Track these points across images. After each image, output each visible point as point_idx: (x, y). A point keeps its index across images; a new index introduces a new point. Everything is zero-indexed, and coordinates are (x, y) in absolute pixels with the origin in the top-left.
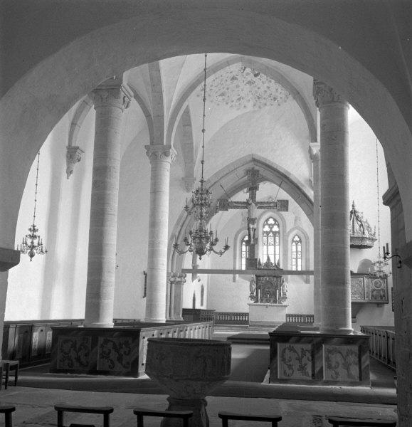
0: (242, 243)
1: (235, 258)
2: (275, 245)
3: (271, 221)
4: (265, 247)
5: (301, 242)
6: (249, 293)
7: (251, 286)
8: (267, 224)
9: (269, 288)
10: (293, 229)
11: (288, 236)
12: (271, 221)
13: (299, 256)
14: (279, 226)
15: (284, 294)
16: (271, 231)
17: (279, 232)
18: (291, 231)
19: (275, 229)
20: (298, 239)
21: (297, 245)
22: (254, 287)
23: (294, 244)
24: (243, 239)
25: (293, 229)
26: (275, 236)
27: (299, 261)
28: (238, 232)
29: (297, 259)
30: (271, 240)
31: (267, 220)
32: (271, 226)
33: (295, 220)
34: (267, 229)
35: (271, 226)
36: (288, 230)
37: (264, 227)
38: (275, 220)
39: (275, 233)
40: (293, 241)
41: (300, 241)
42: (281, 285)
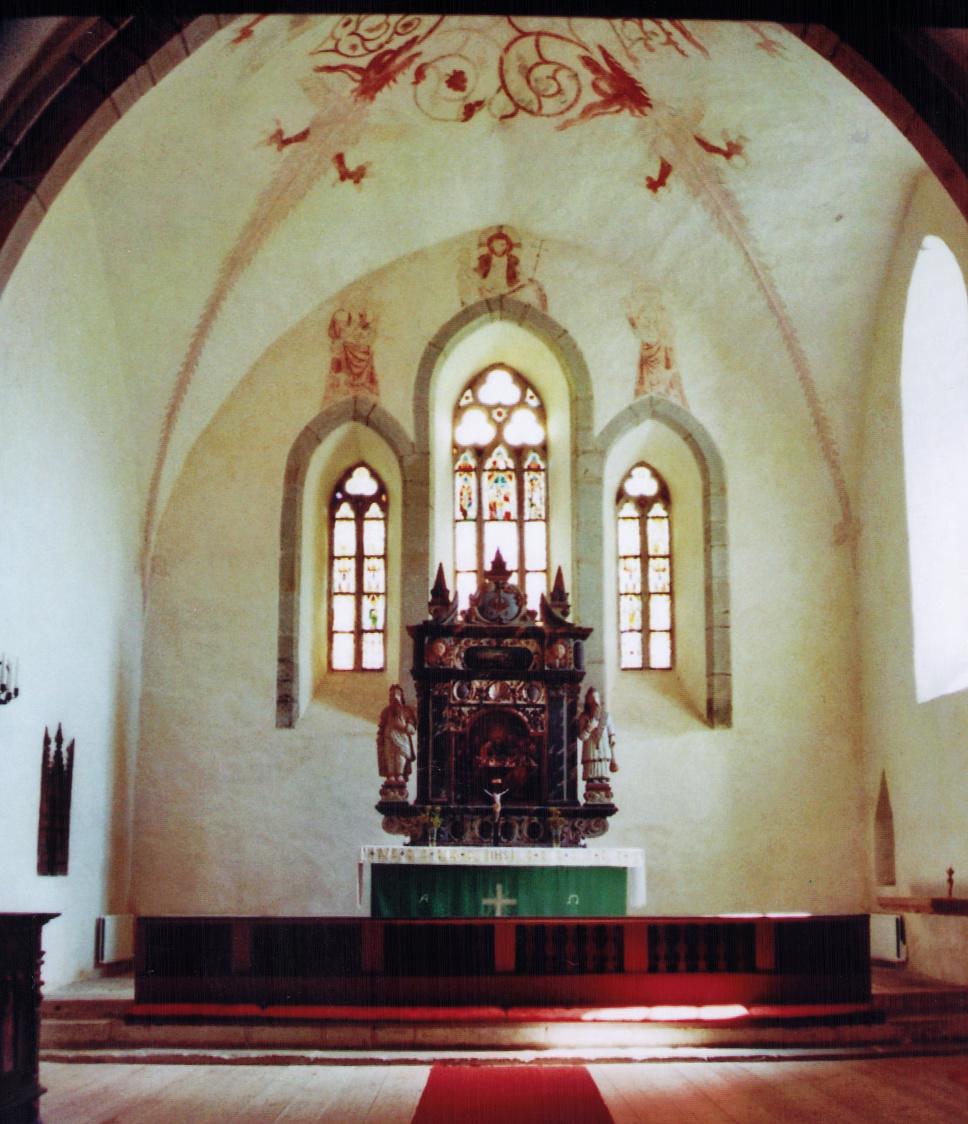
0: (334, 505)
1: (289, 581)
2: (521, 523)
3: (500, 388)
4: (468, 530)
5: (664, 495)
6: (372, 785)
7: (383, 740)
8: (477, 403)
9: (501, 751)
10: (632, 415)
11: (602, 454)
12: (500, 388)
13: (658, 580)
14: (542, 412)
15: (598, 785)
16: (498, 441)
17: (543, 449)
18: (614, 429)
19: (524, 429)
20: (650, 488)
21: (643, 520)
22: (408, 743)
23: (629, 509)
24: (340, 486)
25: (632, 415)
26: (519, 472)
27: (660, 608)
28: (310, 437)
29: (645, 595)
30: (499, 491)
31: (474, 383)
32: (499, 415)
33: (645, 363)
34: (476, 429)
35: (499, 415)
36: (601, 420)
37: (458, 411)
38: (522, 381)
39: (518, 453)
40: (621, 496)
41: (664, 495)
42: (575, 731)
